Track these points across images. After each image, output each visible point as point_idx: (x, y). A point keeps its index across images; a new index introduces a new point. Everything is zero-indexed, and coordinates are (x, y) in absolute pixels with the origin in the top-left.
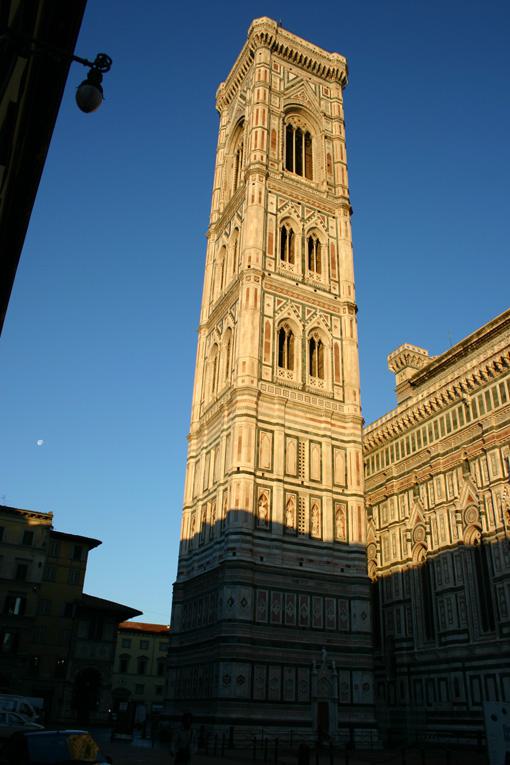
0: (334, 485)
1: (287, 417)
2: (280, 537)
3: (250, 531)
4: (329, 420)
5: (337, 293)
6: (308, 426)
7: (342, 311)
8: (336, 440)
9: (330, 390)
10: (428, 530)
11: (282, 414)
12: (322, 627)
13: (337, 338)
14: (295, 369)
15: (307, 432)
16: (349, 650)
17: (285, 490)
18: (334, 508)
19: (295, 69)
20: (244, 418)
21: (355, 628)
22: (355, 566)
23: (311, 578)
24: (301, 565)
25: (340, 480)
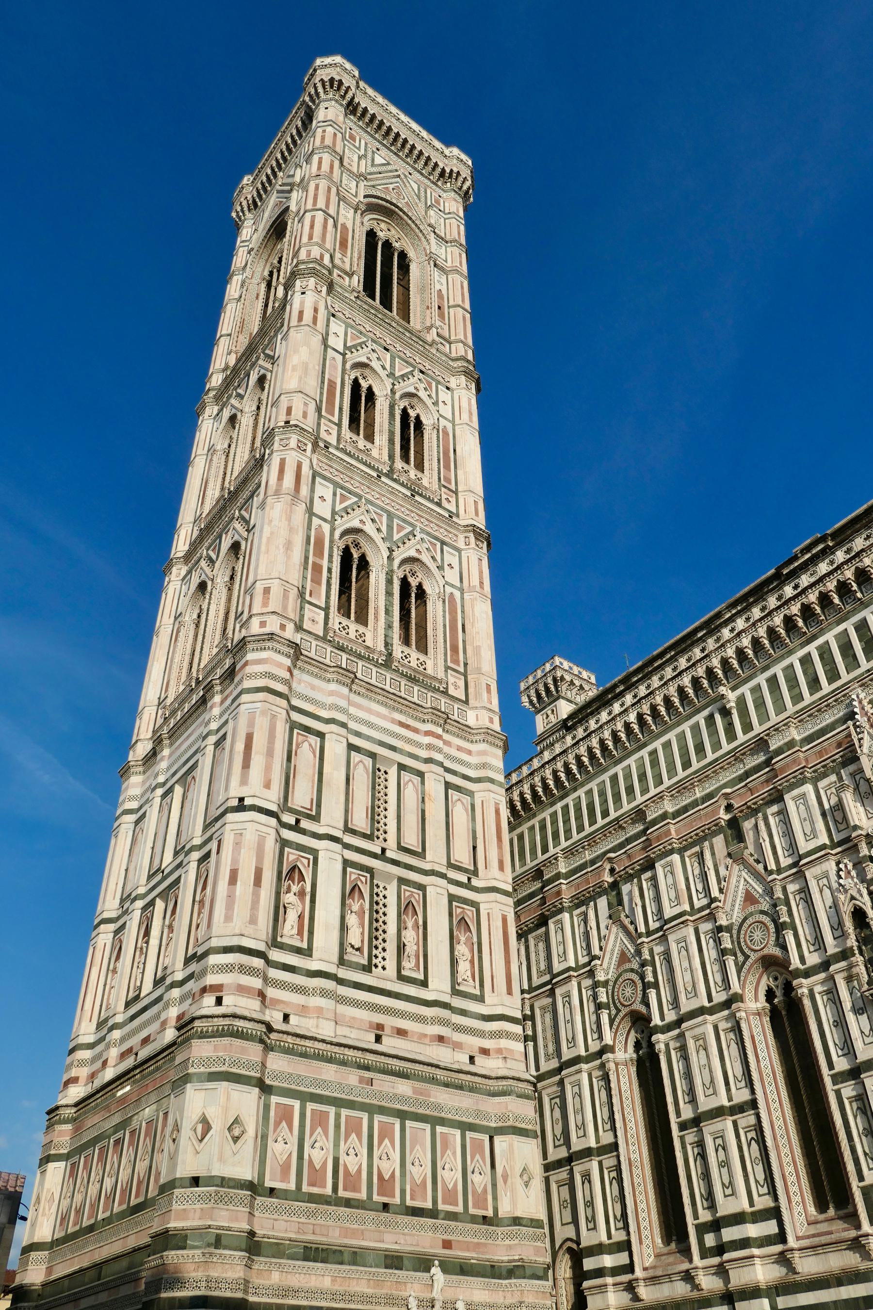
0: (450, 865)
1: (352, 710)
4: (439, 731)
5: (454, 510)
8: (454, 773)
11: (343, 703)
12: (429, 1205)
13: (452, 586)
15: (393, 748)
17: (346, 863)
18: (451, 915)
19: (384, 152)
20: (261, 696)
21: (505, 1210)
22: (499, 1051)
23: (403, 1075)
25: (462, 855)
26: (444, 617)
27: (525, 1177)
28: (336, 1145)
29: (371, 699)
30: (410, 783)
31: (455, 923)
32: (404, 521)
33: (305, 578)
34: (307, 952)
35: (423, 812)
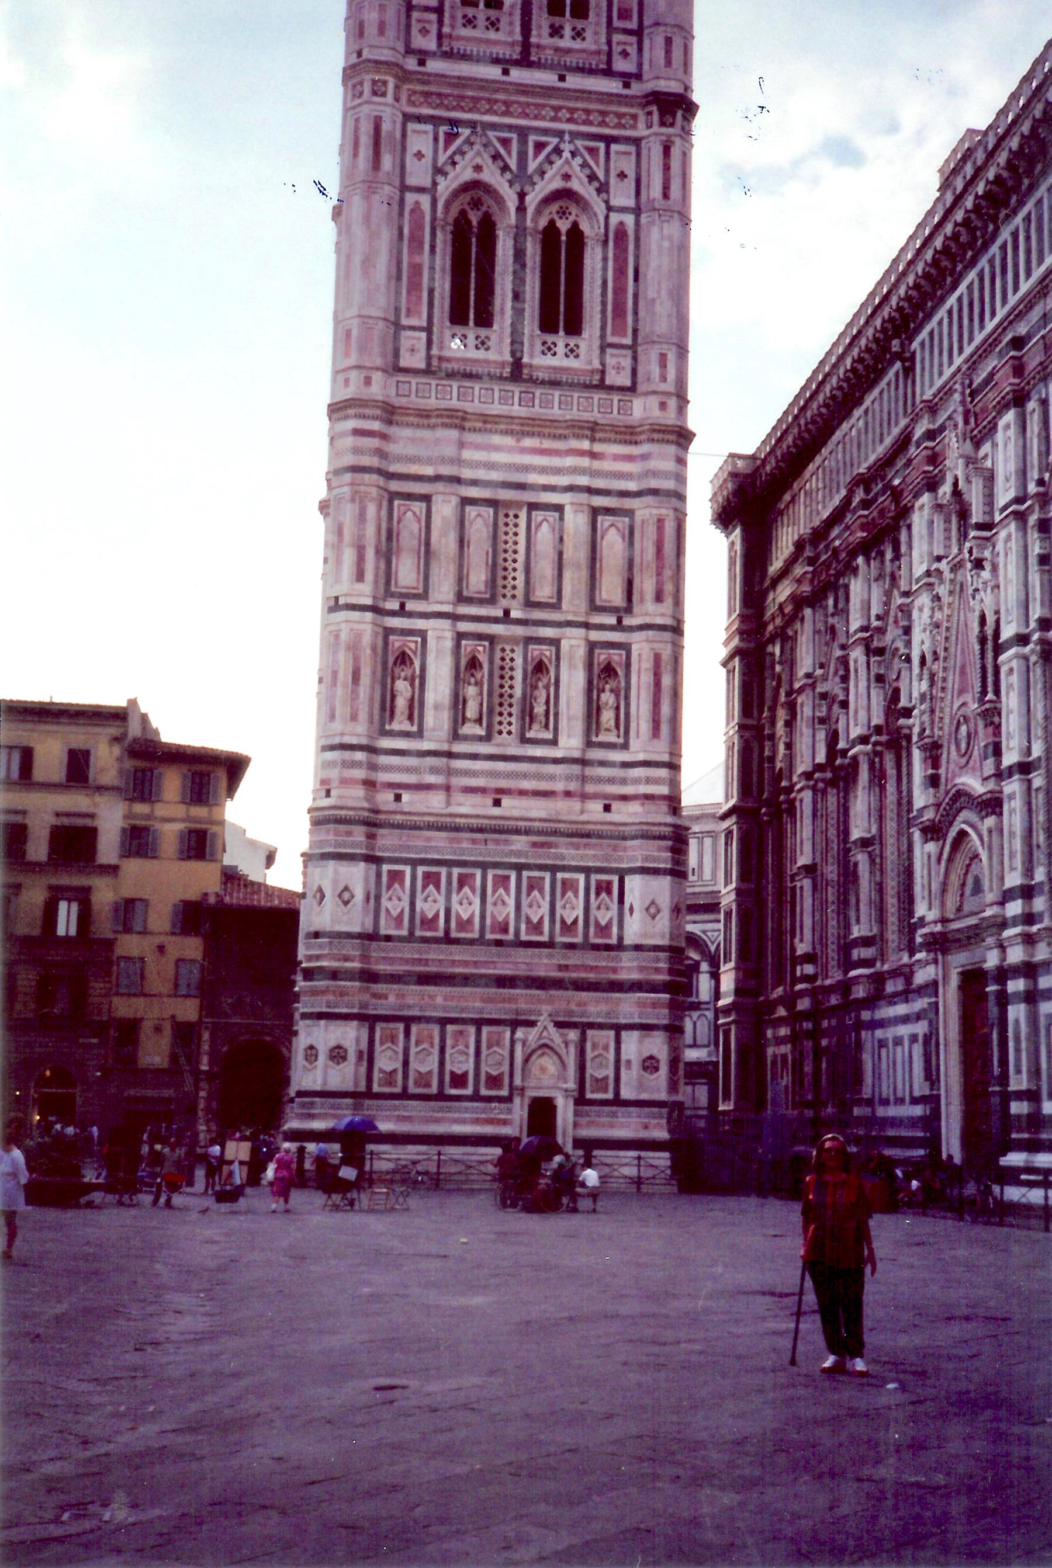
0: (595, 608)
1: (467, 454)
2: (445, 747)
3: (364, 741)
4: (586, 445)
6: (526, 469)
7: (641, 125)
9: (597, 365)
10: (841, 697)
11: (450, 451)
13: (623, 210)
14: (495, 327)
16: (616, 986)
17: (460, 636)
18: (590, 666)
24: (497, 803)
25: (611, 591)
26: (605, 269)
27: (653, 910)
28: (448, 898)
29: (490, 431)
30: (545, 524)
31: (596, 670)
32: (546, 132)
33: (398, 293)
34: (420, 734)
35: (560, 554)
